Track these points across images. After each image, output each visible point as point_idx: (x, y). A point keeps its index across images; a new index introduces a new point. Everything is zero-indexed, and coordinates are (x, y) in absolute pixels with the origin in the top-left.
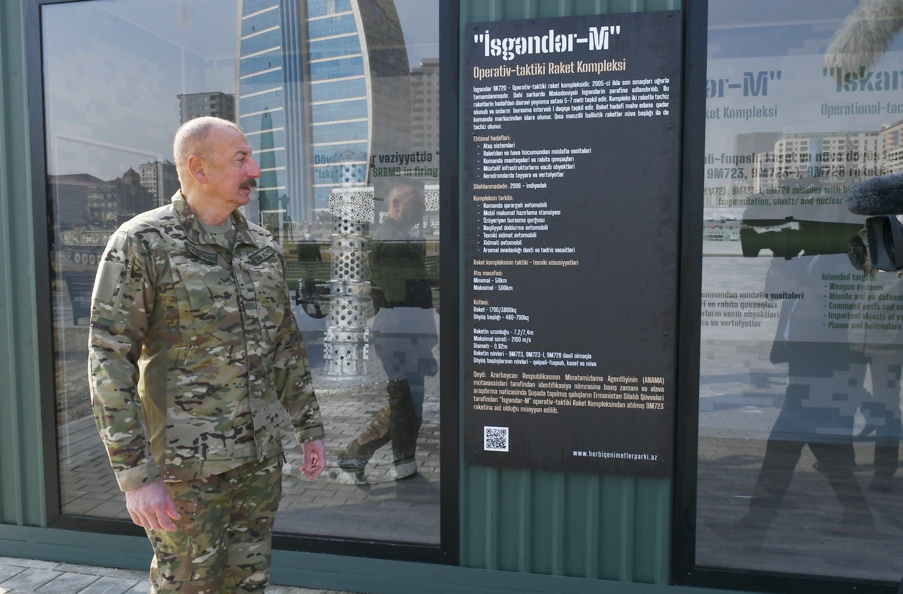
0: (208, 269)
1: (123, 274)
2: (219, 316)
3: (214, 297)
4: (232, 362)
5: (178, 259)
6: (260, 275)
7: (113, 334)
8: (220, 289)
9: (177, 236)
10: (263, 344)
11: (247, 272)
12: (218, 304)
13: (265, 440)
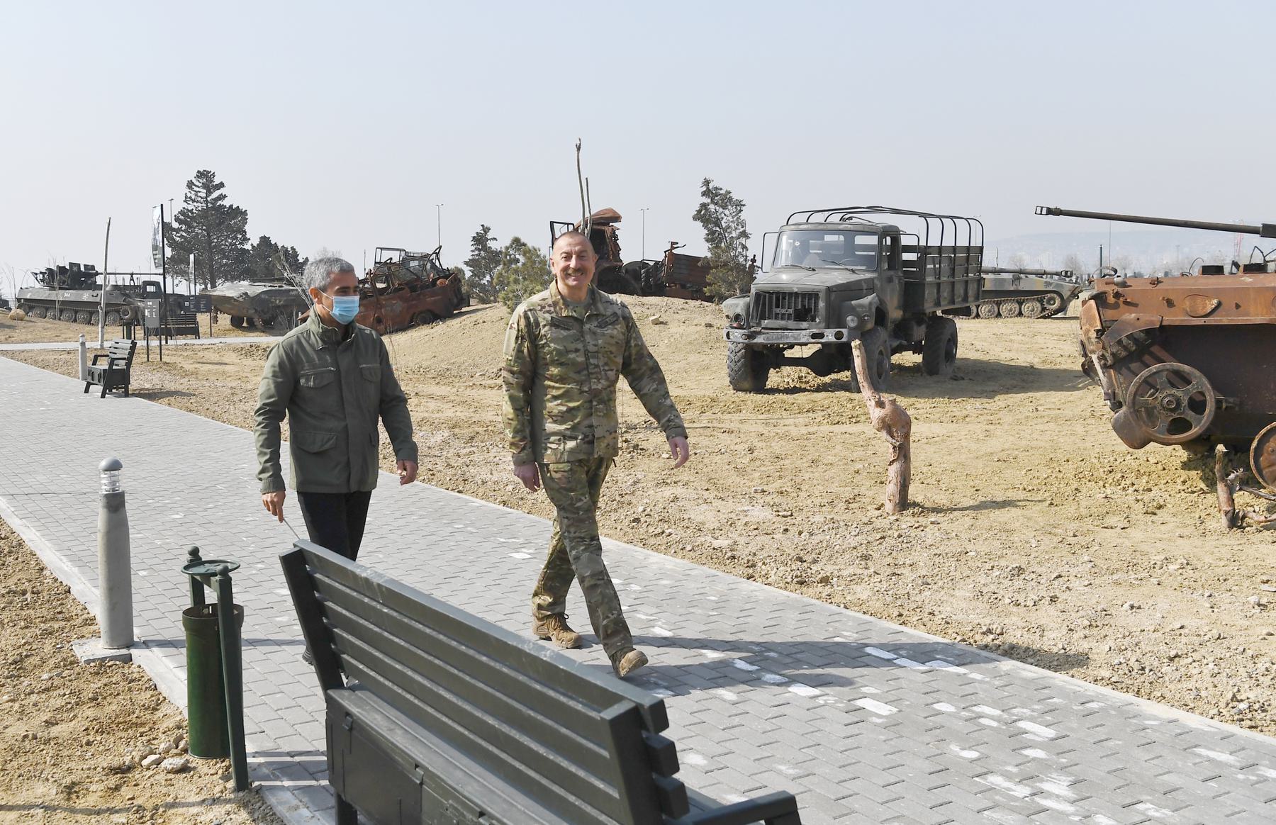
0: (564, 333)
2: (574, 363)
3: (568, 352)
6: (604, 335)
8: (572, 346)
9: (548, 312)
11: (594, 333)
12: (572, 356)
13: (603, 445)
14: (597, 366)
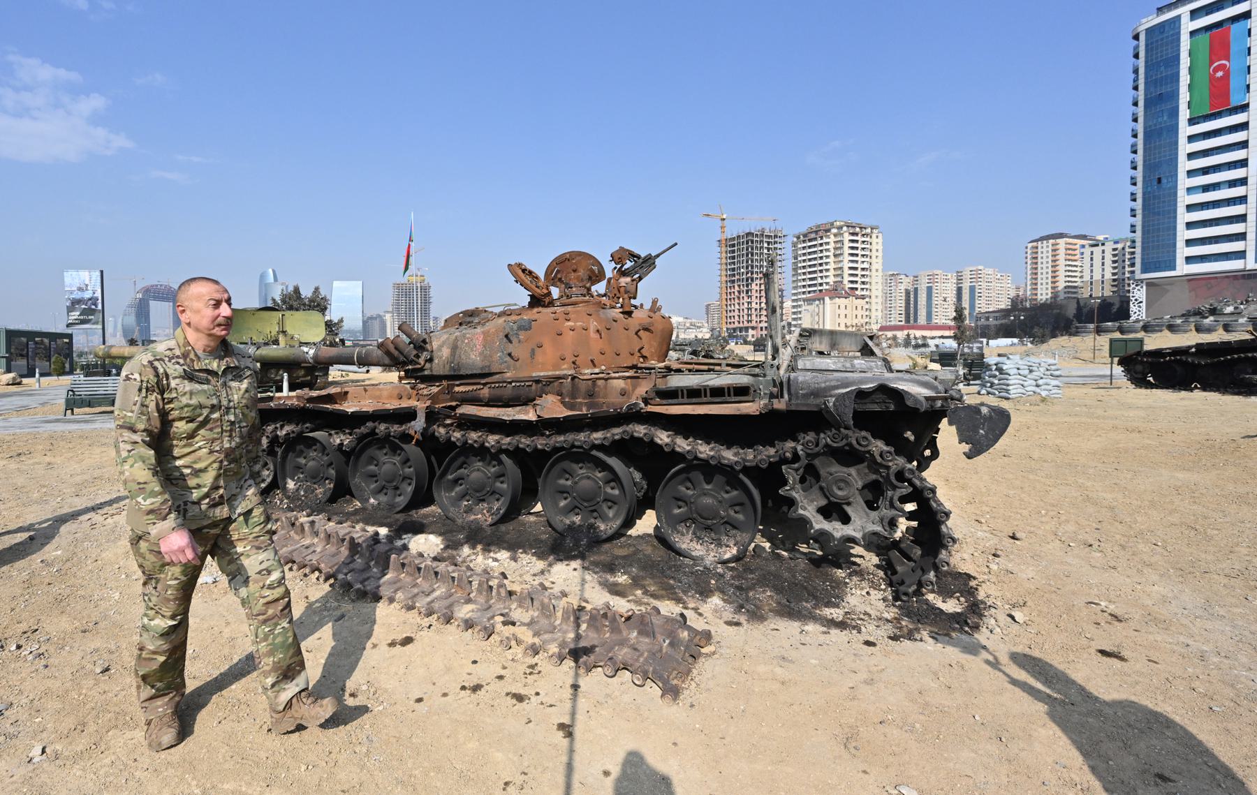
0: (198, 387)
1: (140, 390)
4: (211, 452)
5: (177, 381)
7: (135, 432)
10: (237, 440)
14: (232, 423)
